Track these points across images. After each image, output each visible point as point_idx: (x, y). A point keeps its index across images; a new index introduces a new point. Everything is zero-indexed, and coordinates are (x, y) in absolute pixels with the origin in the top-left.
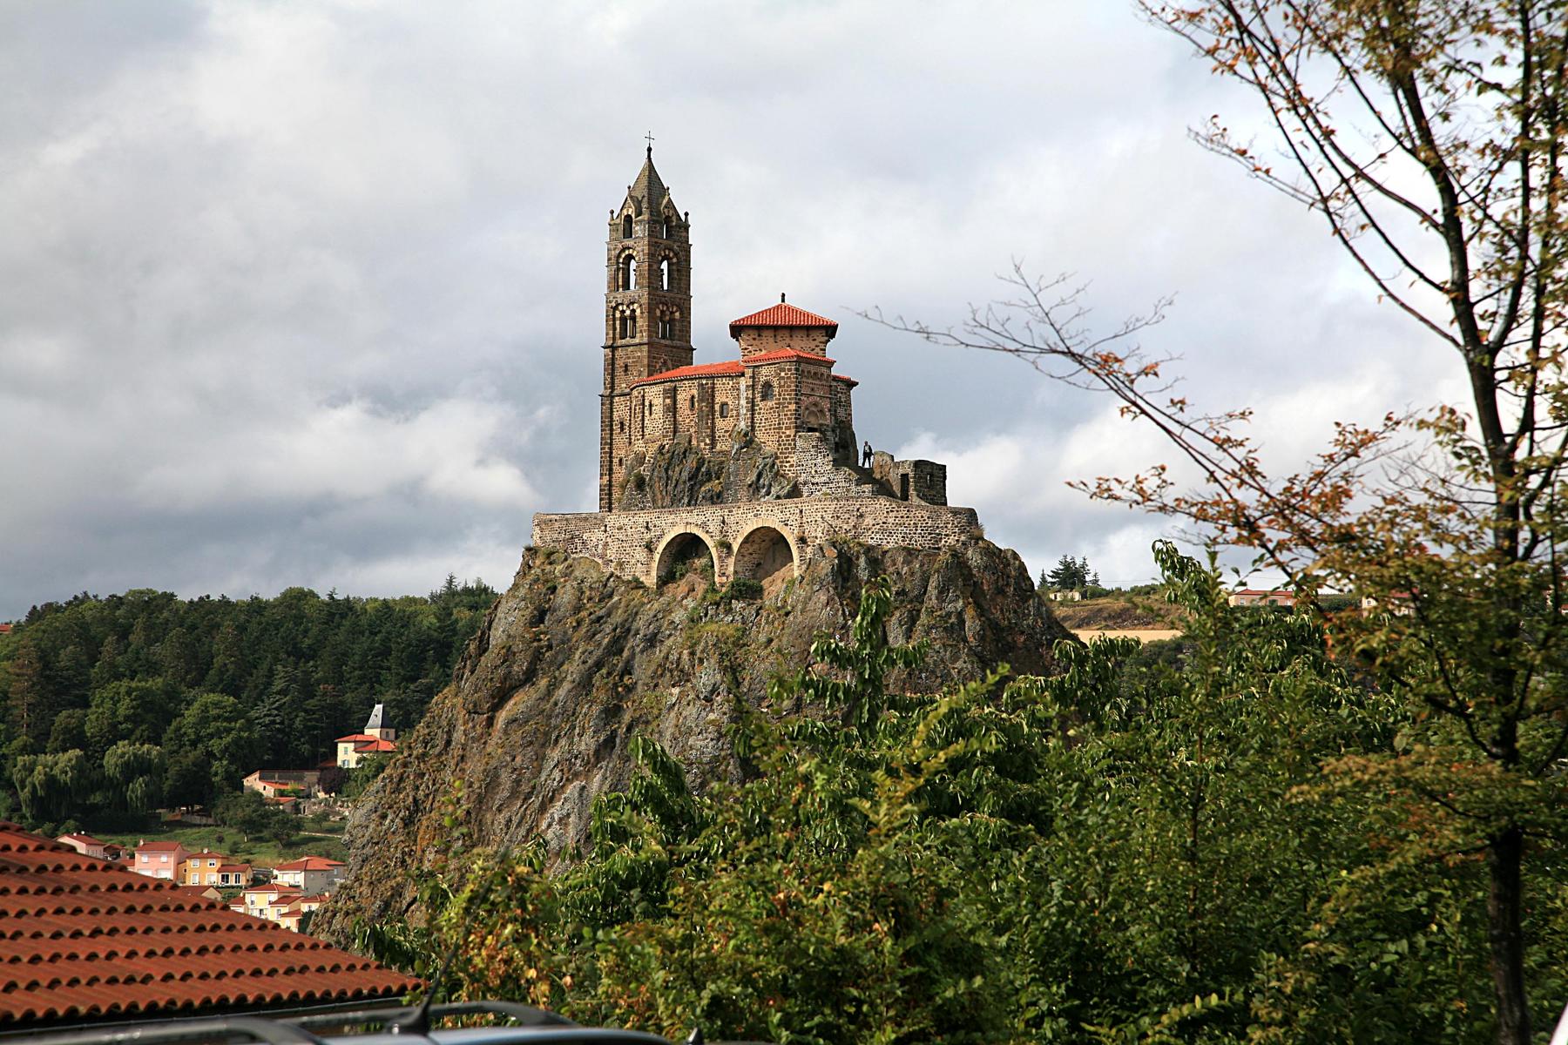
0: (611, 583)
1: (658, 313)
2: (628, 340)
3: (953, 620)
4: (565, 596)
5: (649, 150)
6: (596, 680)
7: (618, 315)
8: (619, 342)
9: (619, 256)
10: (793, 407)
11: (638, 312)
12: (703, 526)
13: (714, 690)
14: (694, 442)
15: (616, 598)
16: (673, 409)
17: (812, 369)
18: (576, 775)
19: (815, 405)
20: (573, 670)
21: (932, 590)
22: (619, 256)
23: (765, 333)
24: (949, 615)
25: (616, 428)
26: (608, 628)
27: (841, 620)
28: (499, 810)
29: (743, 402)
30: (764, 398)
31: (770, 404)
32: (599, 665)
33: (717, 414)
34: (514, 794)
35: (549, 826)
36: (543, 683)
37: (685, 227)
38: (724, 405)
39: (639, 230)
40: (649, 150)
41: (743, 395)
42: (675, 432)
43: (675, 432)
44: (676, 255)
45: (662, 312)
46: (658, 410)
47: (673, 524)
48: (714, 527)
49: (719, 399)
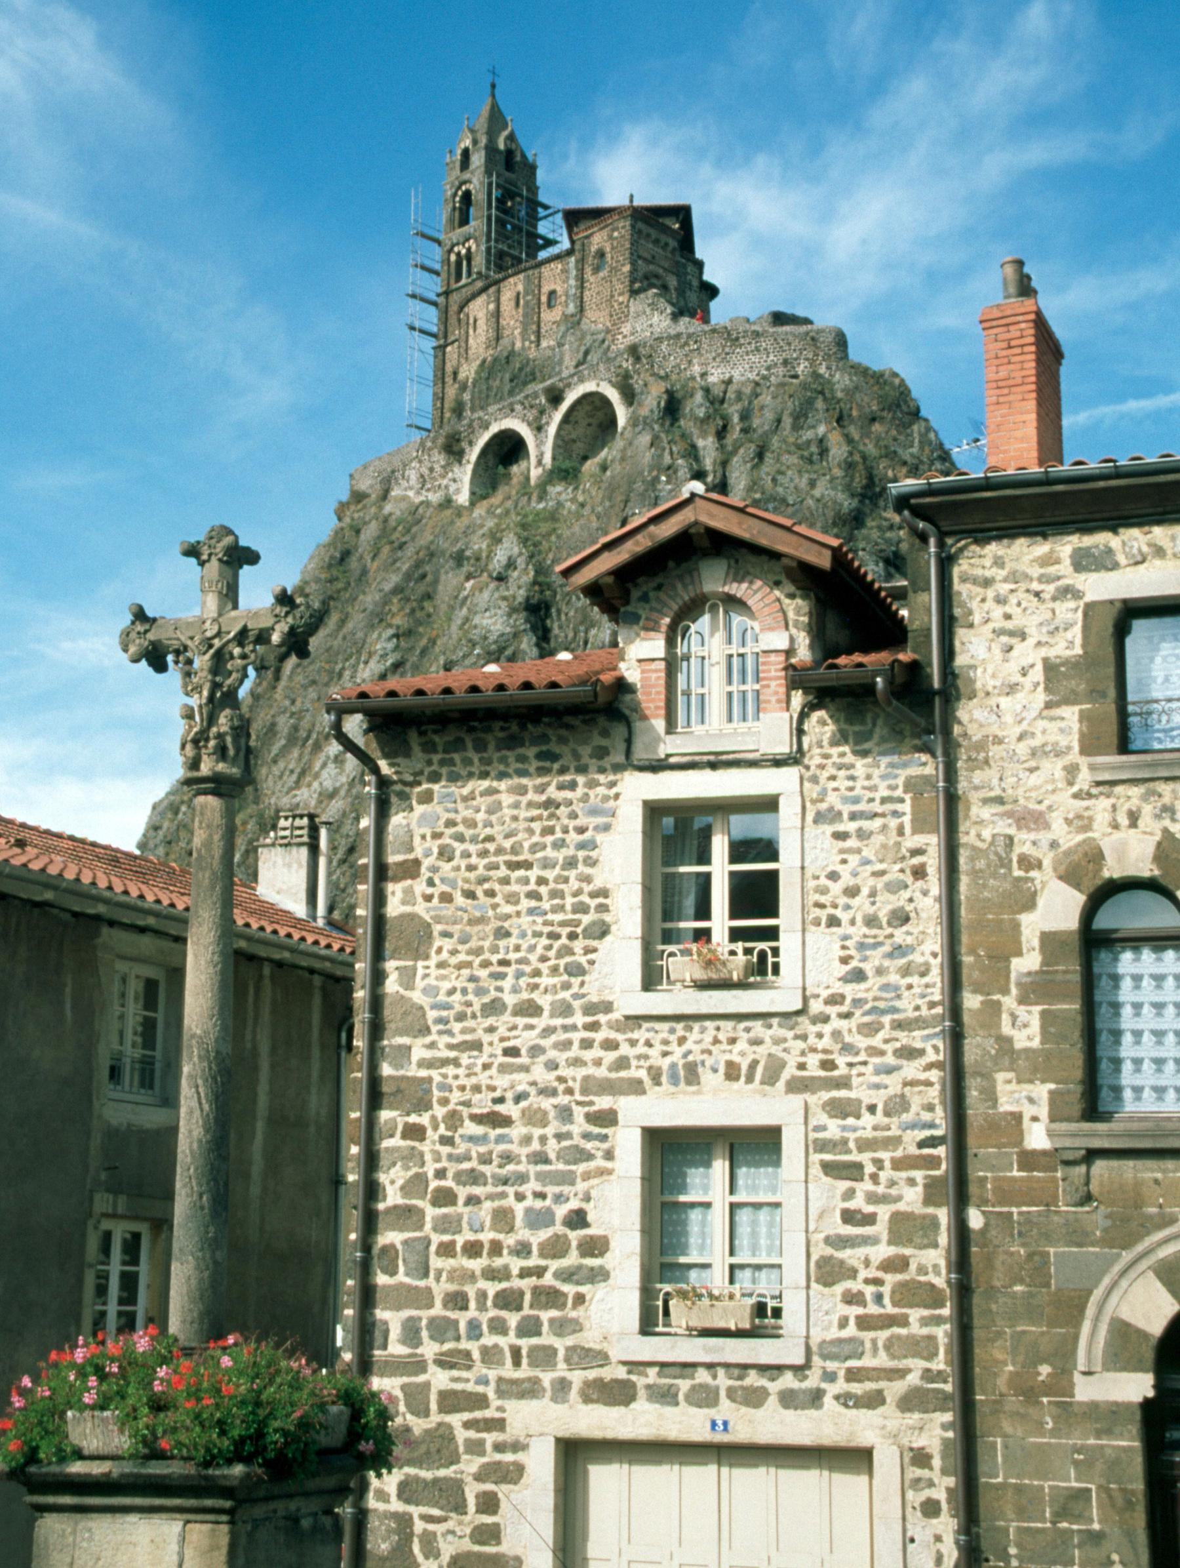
0: (421, 510)
2: (464, 281)
3: (814, 449)
4: (370, 531)
5: (493, 86)
7: (453, 258)
8: (454, 286)
9: (455, 195)
10: (627, 268)
11: (474, 248)
13: (511, 564)
14: (518, 345)
16: (497, 314)
20: (370, 599)
21: (787, 421)
22: (455, 195)
24: (809, 442)
25: (449, 380)
26: (410, 551)
27: (667, 459)
28: (275, 761)
29: (572, 282)
30: (597, 270)
31: (601, 274)
32: (397, 590)
33: (544, 307)
34: (292, 740)
35: (324, 765)
36: (333, 620)
37: (532, 168)
38: (552, 293)
39: (478, 160)
40: (493, 86)
42: (498, 339)
43: (498, 339)
46: (481, 323)
49: (546, 289)
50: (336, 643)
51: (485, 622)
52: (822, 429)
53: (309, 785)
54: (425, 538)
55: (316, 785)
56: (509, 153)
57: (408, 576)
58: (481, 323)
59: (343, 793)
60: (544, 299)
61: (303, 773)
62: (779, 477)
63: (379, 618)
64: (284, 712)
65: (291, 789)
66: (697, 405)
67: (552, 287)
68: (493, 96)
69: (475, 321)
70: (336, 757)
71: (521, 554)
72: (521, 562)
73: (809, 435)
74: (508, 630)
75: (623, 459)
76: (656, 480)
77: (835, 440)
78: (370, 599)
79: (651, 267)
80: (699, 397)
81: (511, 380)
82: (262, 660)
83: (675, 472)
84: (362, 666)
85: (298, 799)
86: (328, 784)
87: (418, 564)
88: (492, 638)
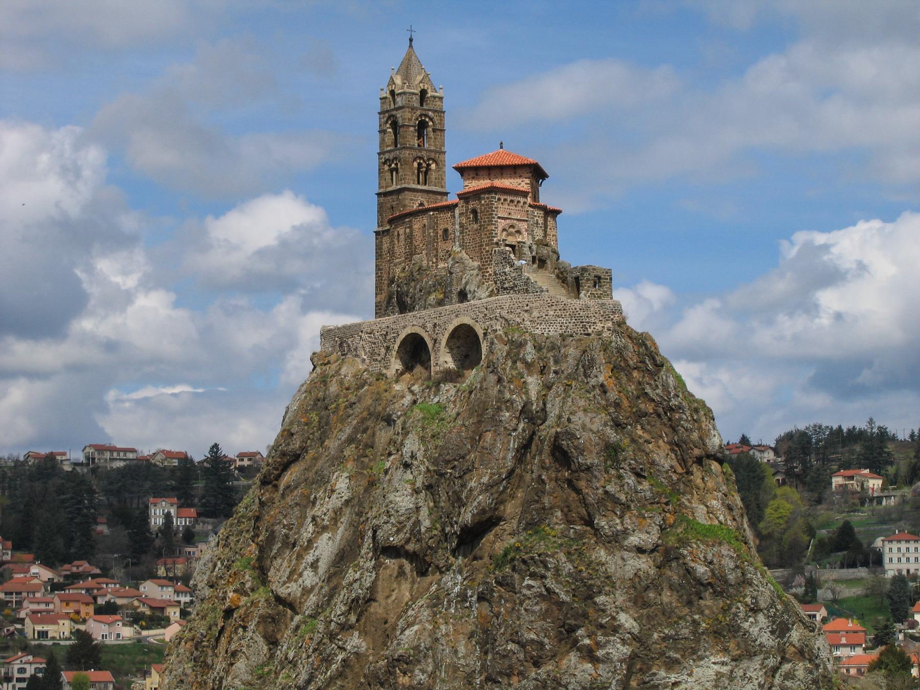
1: (415, 165)
3: (598, 391)
5: (411, 40)
6: (347, 453)
12: (424, 327)
15: (366, 388)
17: (509, 198)
18: (325, 529)
19: (512, 226)
23: (480, 173)
29: (457, 227)
32: (350, 440)
36: (308, 457)
40: (411, 40)
41: (458, 221)
43: (412, 255)
44: (431, 119)
45: (419, 164)
46: (402, 237)
47: (404, 327)
48: (429, 326)
50: (311, 474)
51: (398, 499)
52: (601, 379)
53: (296, 581)
54: (368, 401)
55: (300, 581)
56: (423, 93)
57: (356, 430)
58: (402, 237)
59: (316, 590)
60: (440, 232)
61: (292, 573)
62: (571, 417)
63: (338, 460)
64: (279, 523)
65: (285, 583)
66: (529, 352)
67: (446, 226)
68: (411, 46)
69: (398, 235)
70: (312, 564)
71: (419, 449)
72: (420, 455)
73: (593, 382)
74: (411, 506)
75: (481, 389)
76: (499, 409)
77: (610, 384)
78: (332, 444)
79: (507, 221)
80: (529, 348)
81: (421, 291)
82: (265, 477)
83: (512, 404)
84: (327, 499)
85: (289, 590)
86: (308, 583)
87: (363, 420)
88: (403, 511)
